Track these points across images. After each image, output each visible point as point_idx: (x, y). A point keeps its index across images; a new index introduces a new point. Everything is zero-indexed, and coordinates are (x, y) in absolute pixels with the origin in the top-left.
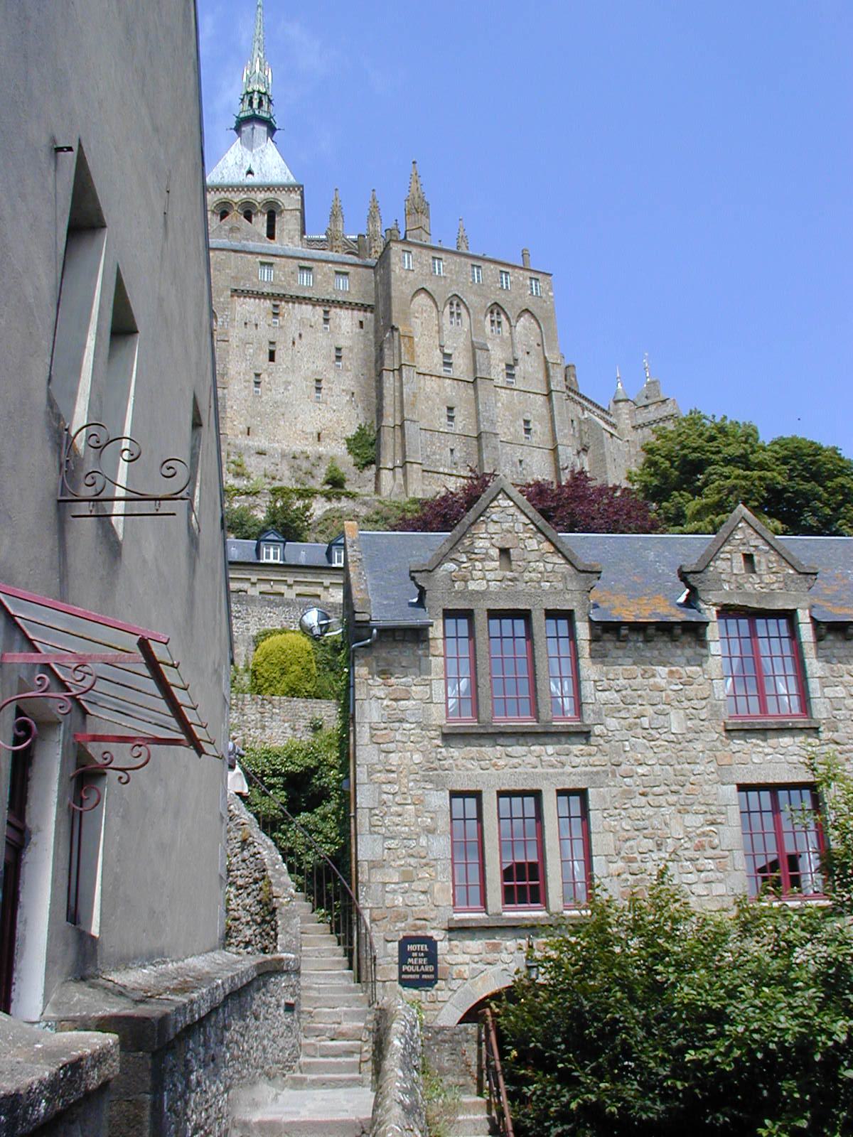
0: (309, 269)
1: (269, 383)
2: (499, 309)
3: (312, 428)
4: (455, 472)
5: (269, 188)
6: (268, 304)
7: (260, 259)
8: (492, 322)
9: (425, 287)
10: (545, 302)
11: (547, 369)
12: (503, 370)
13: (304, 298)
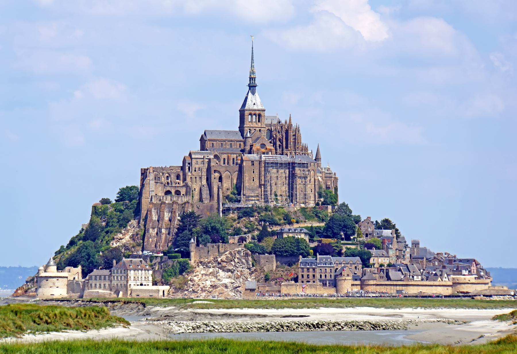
5: (259, 110)
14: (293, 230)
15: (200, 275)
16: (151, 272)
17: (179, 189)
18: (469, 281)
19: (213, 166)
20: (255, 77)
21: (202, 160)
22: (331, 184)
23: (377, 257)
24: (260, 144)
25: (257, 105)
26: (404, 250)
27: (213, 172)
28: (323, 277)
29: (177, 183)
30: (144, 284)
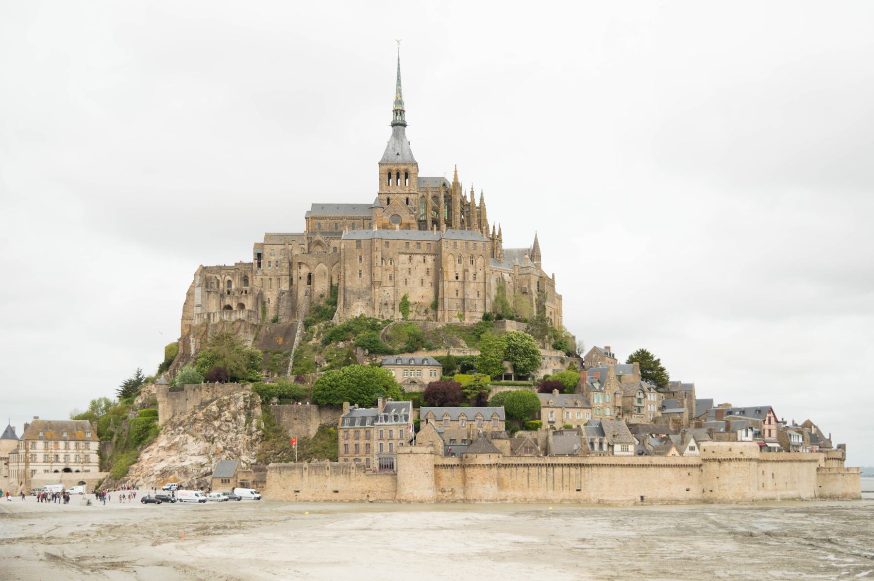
3: (421, 295)
6: (408, 256)
14: (406, 362)
15: (156, 449)
16: (95, 446)
17: (243, 302)
18: (741, 453)
21: (283, 247)
22: (529, 286)
23: (561, 407)
24: (390, 216)
25: (403, 156)
26: (642, 396)
27: (295, 266)
28: (386, 450)
29: (244, 292)
30: (74, 469)
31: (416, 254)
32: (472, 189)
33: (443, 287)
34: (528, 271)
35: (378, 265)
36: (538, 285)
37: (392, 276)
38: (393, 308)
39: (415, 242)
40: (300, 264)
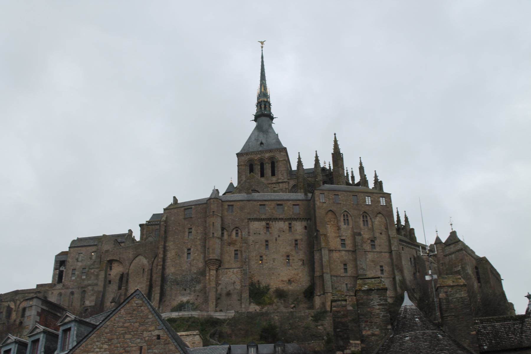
0: (281, 205)
1: (266, 260)
2: (366, 214)
3: (286, 279)
4: (348, 294)
5: (271, 151)
6: (264, 223)
7: (260, 203)
8: (363, 221)
9: (331, 209)
10: (388, 208)
11: (389, 241)
12: (369, 244)
13: (280, 219)
19: (107, 251)
20: (265, 100)
21: (94, 249)
22: (462, 268)
31: (276, 219)
32: (361, 164)
33: (321, 259)
34: (459, 247)
35: (215, 235)
36: (477, 273)
37: (239, 253)
38: (240, 300)
39: (273, 204)
40: (111, 262)
